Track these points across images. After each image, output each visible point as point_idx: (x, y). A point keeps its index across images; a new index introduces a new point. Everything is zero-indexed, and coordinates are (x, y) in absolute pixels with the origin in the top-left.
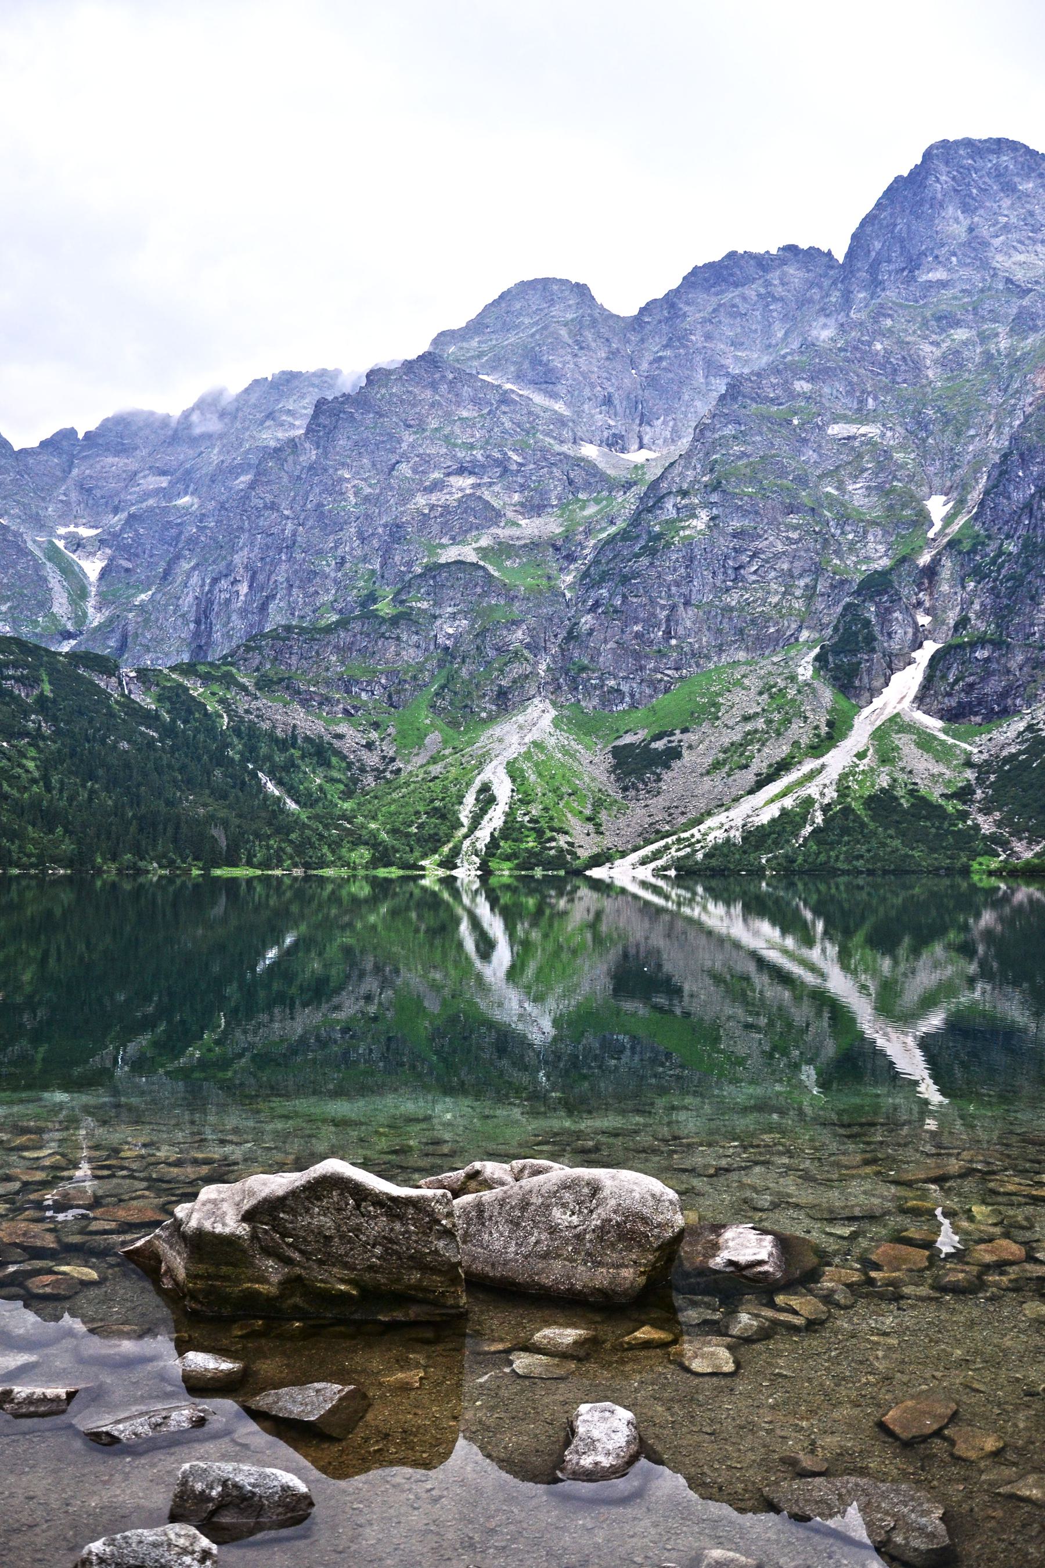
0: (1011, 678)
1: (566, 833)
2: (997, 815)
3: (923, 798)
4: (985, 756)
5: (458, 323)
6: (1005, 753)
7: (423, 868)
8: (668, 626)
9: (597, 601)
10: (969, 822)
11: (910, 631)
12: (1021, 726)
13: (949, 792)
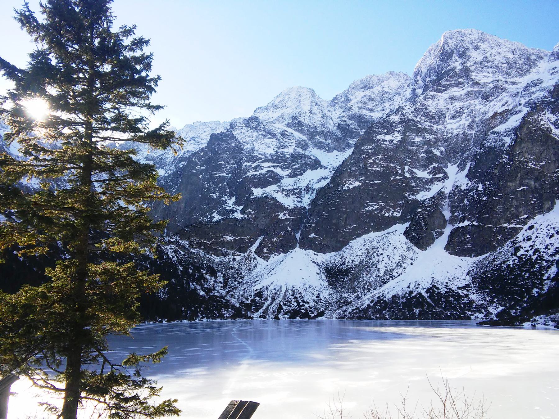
1: (308, 303)
3: (450, 289)
5: (264, 105)
7: (252, 318)
8: (346, 220)
9: (319, 211)
11: (442, 221)
13: (461, 286)
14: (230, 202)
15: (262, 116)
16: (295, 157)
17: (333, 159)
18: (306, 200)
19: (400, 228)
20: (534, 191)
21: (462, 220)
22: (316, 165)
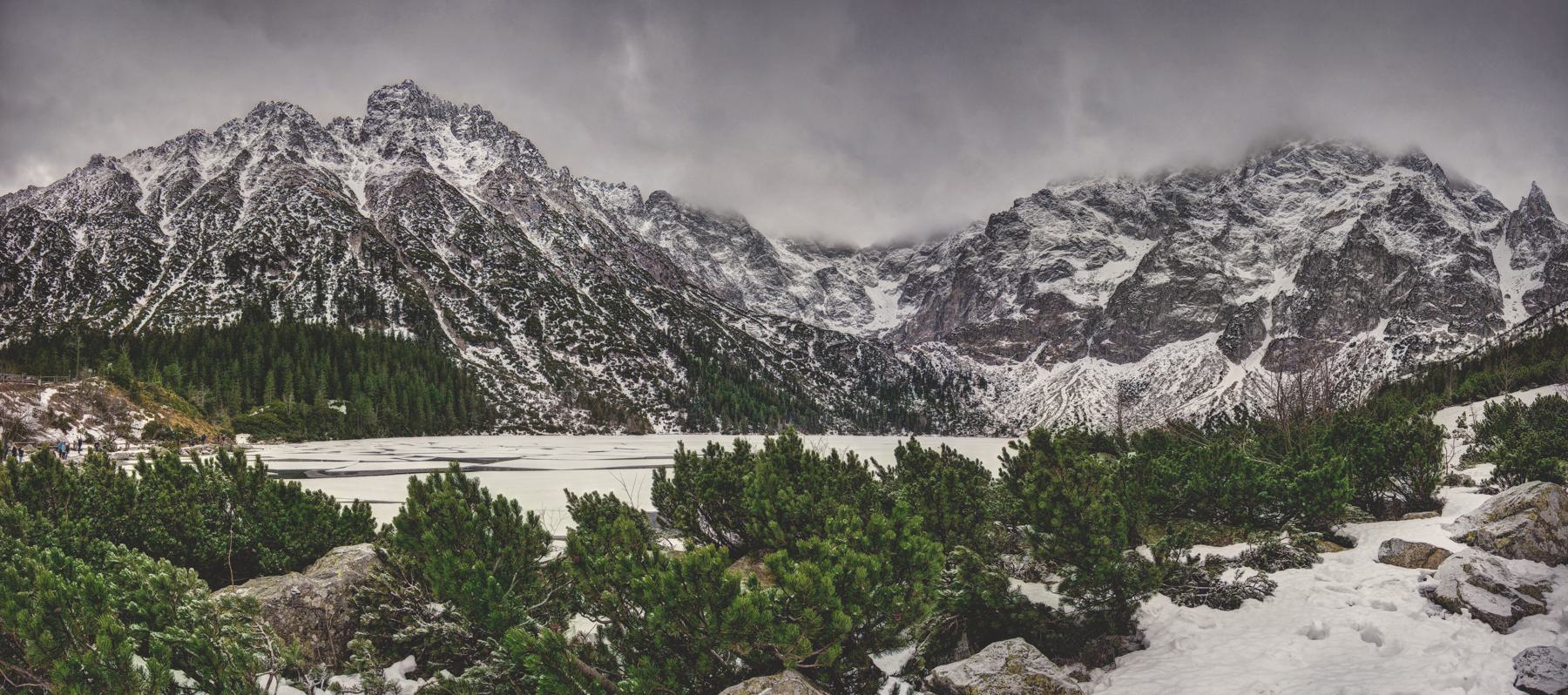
14: (1010, 300)
15: (1057, 192)
16: (1094, 244)
17: (1137, 249)
18: (1104, 299)
19: (1213, 337)
20: (1361, 305)
21: (1283, 330)
22: (1122, 254)
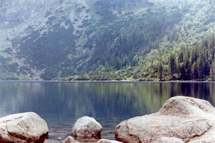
0: (20, 8)
2: (23, 59)
4: (14, 37)
6: (22, 36)
10: (13, 62)
12: (26, 26)
13: (4, 50)
